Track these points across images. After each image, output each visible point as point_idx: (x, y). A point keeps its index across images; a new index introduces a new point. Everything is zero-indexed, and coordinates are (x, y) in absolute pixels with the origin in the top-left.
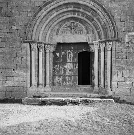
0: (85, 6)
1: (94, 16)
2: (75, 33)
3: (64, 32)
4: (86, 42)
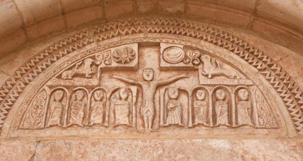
2: (174, 118)
3: (67, 112)
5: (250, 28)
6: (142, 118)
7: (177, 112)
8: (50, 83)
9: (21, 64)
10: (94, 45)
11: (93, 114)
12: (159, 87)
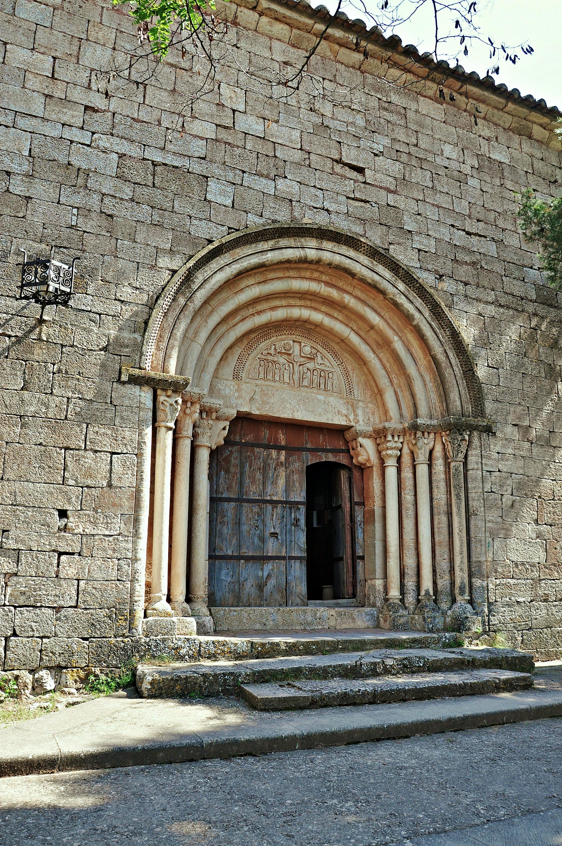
0: (374, 287)
1: (394, 330)
2: (306, 383)
3: (266, 373)
4: (344, 423)
5: (338, 343)
6: (294, 380)
7: (306, 380)
8: (258, 356)
9: (246, 343)
10: (275, 338)
11: (276, 376)
12: (300, 365)
